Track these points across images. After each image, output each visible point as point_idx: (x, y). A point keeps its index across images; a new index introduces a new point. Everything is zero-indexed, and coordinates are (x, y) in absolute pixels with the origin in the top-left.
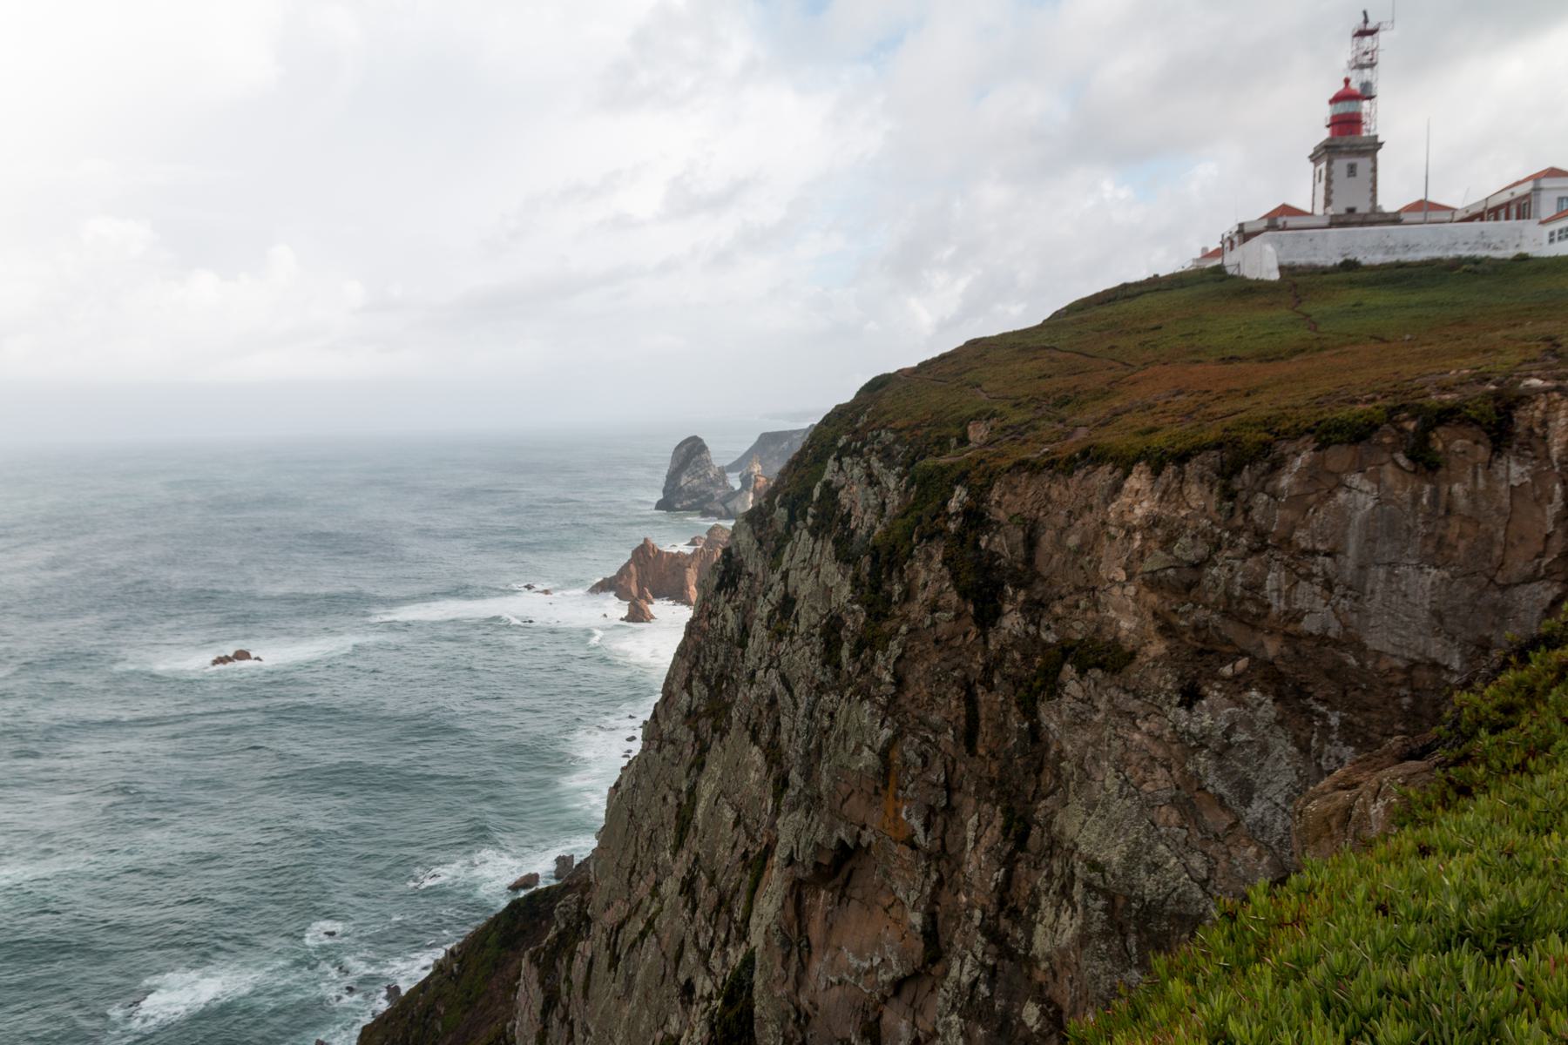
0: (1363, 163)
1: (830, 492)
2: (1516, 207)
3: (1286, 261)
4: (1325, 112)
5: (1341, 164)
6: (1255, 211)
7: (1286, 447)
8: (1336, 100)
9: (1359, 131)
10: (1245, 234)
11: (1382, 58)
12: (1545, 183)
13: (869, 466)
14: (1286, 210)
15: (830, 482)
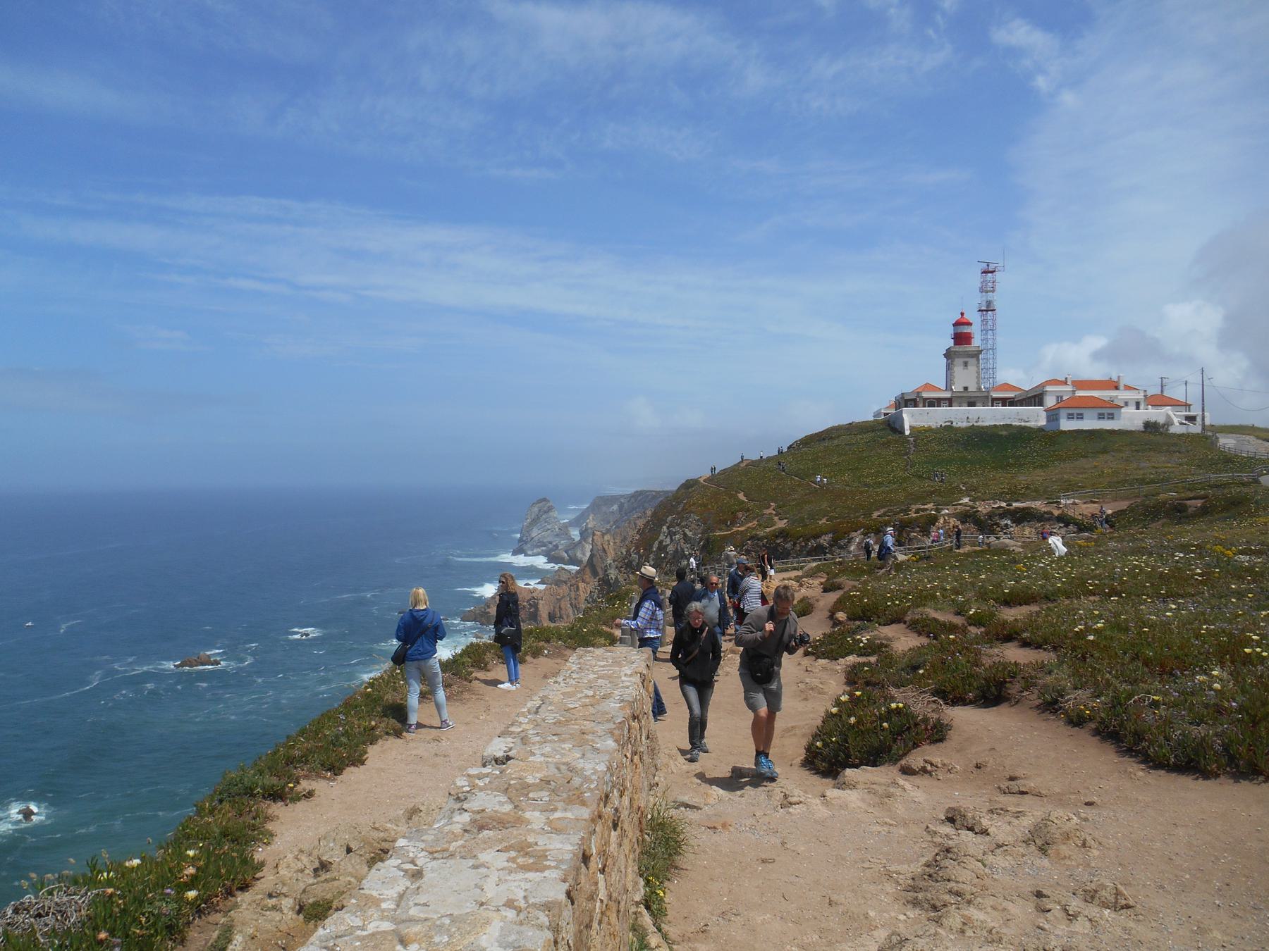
0: (972, 361)
1: (662, 548)
2: (1035, 398)
3: (914, 424)
4: (951, 330)
5: (959, 362)
6: (909, 388)
7: (854, 534)
8: (957, 324)
9: (969, 343)
10: (906, 401)
11: (998, 287)
12: (1048, 388)
13: (685, 534)
14: (928, 387)
15: (661, 542)
